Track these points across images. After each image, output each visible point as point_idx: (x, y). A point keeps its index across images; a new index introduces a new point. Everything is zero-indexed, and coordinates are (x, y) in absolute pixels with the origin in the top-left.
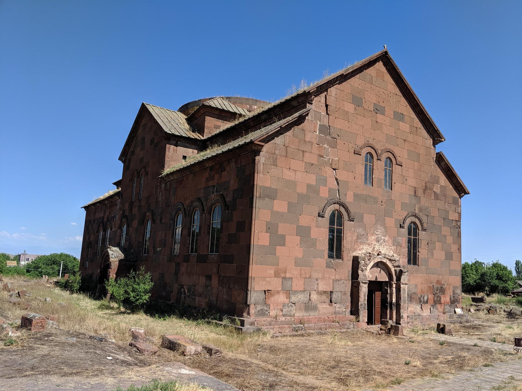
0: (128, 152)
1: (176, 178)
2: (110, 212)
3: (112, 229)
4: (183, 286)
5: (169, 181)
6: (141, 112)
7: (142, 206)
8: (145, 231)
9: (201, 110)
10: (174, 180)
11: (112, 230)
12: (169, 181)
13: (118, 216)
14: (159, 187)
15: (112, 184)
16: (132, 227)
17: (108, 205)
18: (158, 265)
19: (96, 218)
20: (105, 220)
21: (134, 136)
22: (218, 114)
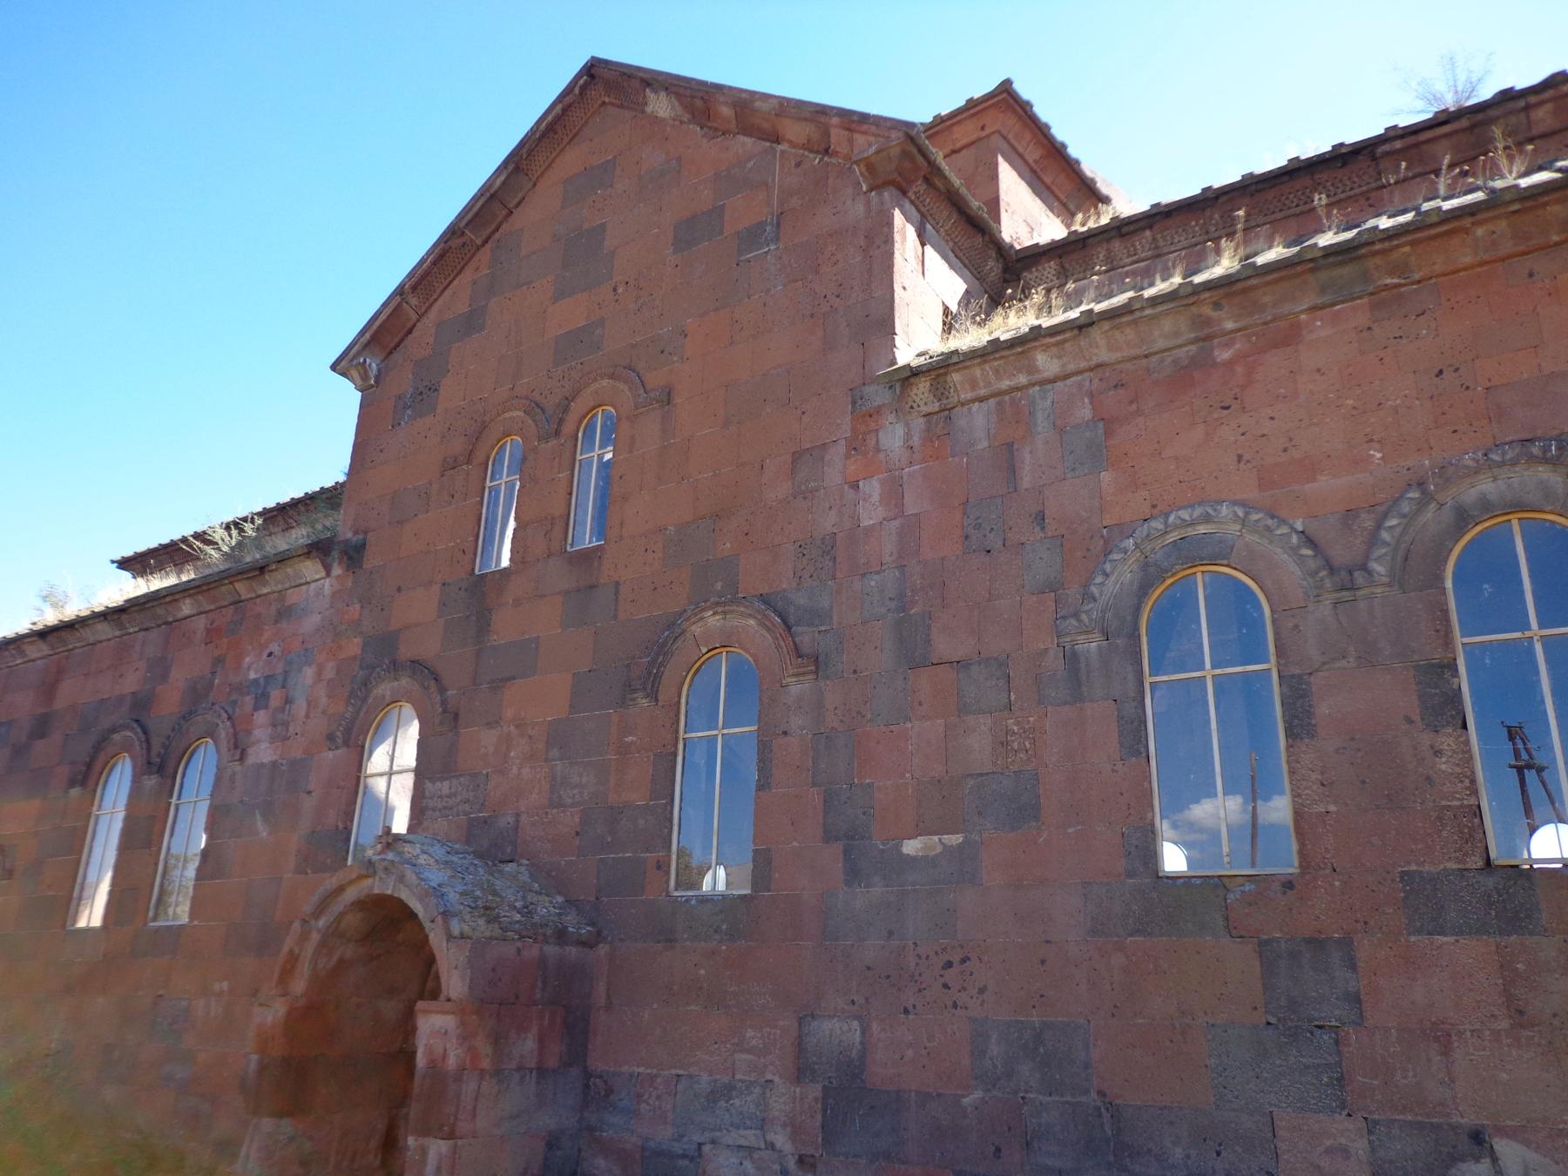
0: (414, 325)
1: (1104, 355)
2: (219, 661)
3: (251, 751)
4: (1477, 1137)
5: (981, 400)
6: (564, 110)
7: (617, 584)
8: (677, 731)
9: (955, 129)
10: (1066, 377)
11: (251, 759)
12: (981, 400)
13: (309, 672)
14: (837, 453)
15: (113, 562)
16: (490, 725)
17: (201, 623)
18: (949, 965)
19: (61, 702)
20: (170, 701)
21: (479, 242)
22: (1033, 164)
